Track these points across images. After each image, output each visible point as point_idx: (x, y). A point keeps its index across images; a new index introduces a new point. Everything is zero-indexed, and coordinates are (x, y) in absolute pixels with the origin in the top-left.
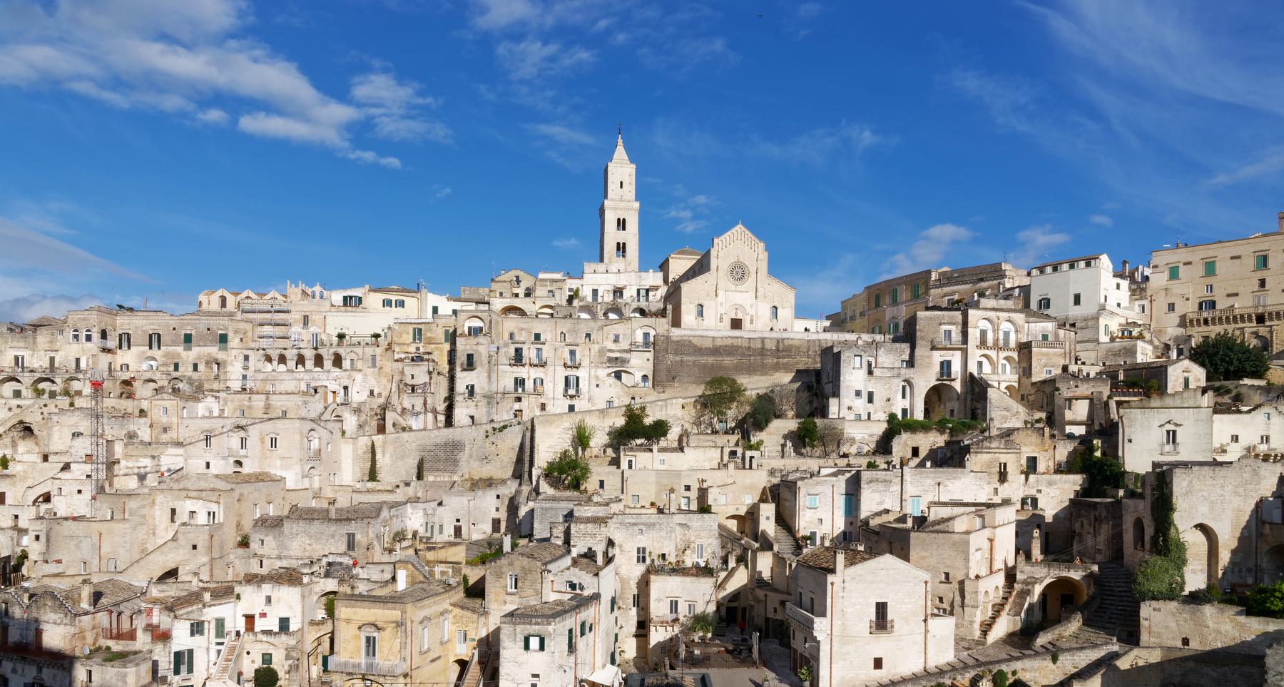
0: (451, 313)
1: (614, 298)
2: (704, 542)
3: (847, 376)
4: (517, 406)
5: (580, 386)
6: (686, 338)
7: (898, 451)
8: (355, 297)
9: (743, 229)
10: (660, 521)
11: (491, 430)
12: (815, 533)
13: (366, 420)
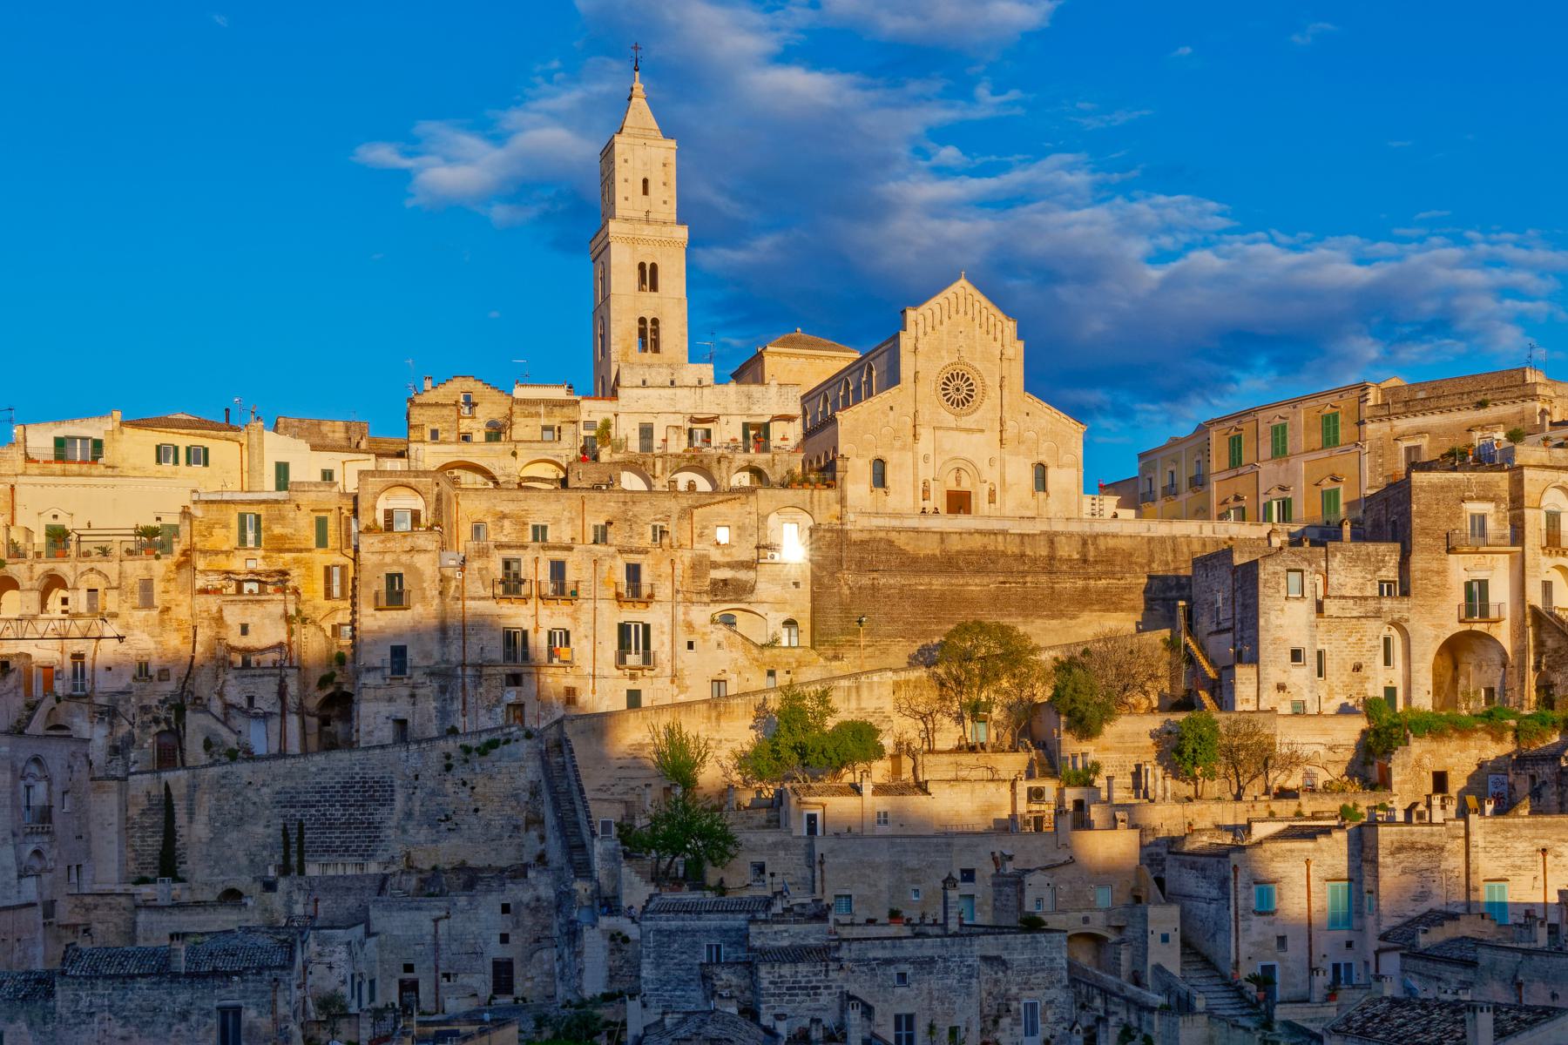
0: (318, 478)
1: (690, 444)
2: (1039, 996)
3: (1272, 617)
4: (511, 695)
5: (654, 646)
6: (882, 535)
7: (1404, 782)
8: (84, 439)
9: (970, 289)
10: (943, 952)
11: (457, 754)
12: (1273, 967)
13: (131, 734)
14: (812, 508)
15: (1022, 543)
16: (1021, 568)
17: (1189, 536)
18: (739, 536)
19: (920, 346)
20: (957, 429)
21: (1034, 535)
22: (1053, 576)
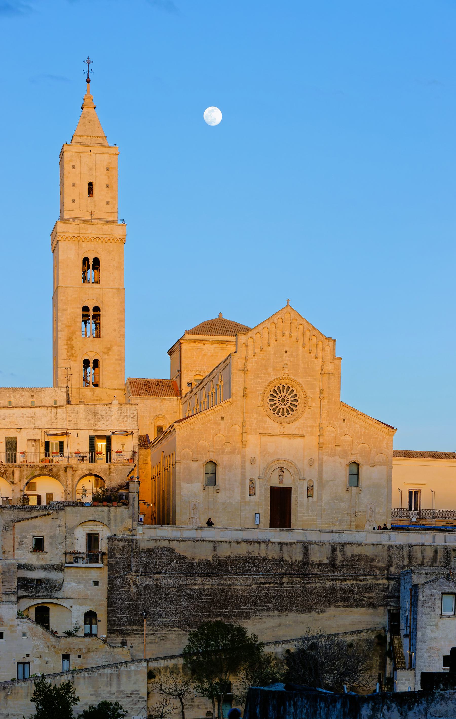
3: (428, 631)
6: (165, 544)
14: (109, 521)
15: (281, 550)
16: (279, 571)
17: (423, 545)
18: (51, 544)
19: (249, 366)
20: (279, 435)
21: (291, 544)
22: (306, 578)
